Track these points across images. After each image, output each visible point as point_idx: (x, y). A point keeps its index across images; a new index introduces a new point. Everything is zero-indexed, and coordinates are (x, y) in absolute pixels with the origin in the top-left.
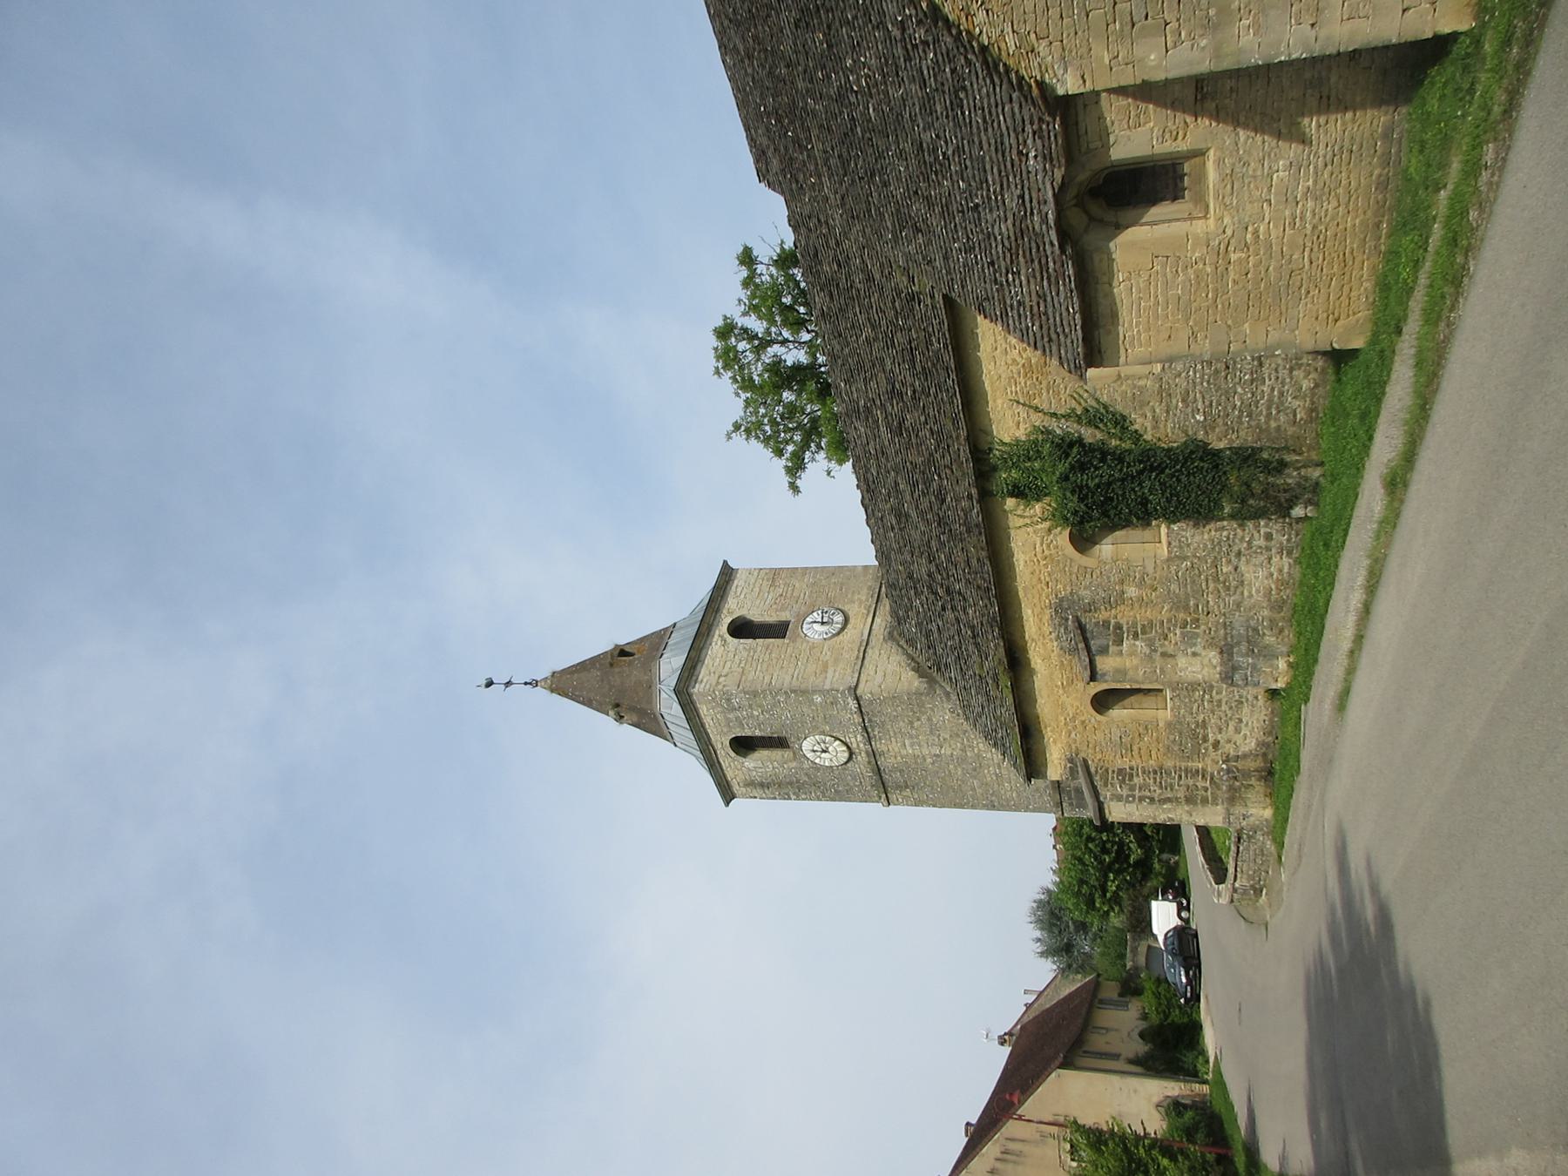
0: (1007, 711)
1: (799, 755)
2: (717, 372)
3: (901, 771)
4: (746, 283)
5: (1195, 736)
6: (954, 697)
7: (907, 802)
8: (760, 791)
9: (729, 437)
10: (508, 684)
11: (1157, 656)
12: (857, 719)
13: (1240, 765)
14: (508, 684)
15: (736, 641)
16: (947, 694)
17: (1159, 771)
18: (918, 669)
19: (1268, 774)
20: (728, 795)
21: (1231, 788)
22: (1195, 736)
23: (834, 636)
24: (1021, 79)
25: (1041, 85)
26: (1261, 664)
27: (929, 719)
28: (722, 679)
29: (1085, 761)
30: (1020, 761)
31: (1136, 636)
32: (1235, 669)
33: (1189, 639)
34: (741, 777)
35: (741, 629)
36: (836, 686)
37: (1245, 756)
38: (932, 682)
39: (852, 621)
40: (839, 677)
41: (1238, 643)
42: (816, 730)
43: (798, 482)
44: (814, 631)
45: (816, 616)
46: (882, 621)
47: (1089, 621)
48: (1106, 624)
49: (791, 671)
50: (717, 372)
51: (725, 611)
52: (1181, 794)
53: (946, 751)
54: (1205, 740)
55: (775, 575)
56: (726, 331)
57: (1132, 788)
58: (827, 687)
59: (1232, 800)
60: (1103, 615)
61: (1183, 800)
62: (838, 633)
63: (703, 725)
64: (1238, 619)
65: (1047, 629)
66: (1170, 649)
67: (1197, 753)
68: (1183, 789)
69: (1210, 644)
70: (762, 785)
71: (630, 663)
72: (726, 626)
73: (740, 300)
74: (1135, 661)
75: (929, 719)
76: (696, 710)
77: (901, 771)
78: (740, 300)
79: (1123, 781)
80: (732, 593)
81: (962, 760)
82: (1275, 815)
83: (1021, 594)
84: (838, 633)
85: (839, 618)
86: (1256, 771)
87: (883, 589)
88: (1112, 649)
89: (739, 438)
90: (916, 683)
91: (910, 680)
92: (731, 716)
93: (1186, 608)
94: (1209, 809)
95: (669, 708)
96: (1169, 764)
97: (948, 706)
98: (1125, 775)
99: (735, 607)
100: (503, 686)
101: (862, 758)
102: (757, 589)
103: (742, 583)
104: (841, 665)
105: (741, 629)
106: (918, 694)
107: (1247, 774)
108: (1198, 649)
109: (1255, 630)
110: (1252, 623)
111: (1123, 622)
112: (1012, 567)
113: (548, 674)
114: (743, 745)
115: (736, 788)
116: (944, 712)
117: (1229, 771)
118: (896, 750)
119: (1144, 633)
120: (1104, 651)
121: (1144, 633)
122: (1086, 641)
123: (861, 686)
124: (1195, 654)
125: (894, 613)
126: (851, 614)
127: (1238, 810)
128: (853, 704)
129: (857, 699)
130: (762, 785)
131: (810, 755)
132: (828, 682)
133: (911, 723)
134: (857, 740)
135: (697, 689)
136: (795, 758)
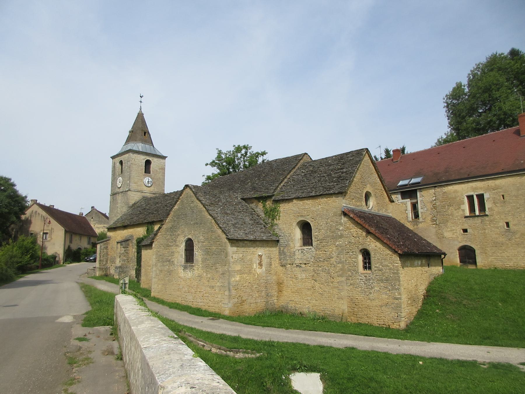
0: (119, 225)
1: (119, 176)
2: (234, 146)
3: (116, 199)
4: (258, 153)
5: (113, 261)
6: (127, 212)
7: (111, 200)
8: (113, 166)
9: (217, 149)
10: (141, 102)
11: (120, 255)
12: (124, 190)
13: (108, 270)
14: (141, 102)
15: (145, 162)
16: (128, 211)
17: (107, 254)
18: (135, 204)
19: (106, 275)
20: (113, 158)
21: (103, 268)
22: (113, 261)
23: (145, 185)
24: (154, 239)
25: (153, 242)
26: (118, 273)
27: (124, 206)
28: (134, 160)
29: (110, 240)
30: (110, 227)
31: (125, 251)
32: (117, 269)
33: (124, 260)
34: (116, 162)
35: (148, 163)
36: (131, 186)
37: (110, 271)
38: (131, 207)
39: (149, 188)
40: (133, 186)
41: (122, 269)
42: (123, 180)
43: (209, 166)
44: (146, 180)
45: (150, 180)
46: (148, 195)
47: (129, 242)
48: (129, 245)
49: (135, 175)
50: (234, 146)
51: (153, 158)
52: (102, 259)
53: (119, 209)
54: (113, 263)
55: (163, 169)
56: (245, 147)
57: (103, 249)
58: (131, 184)
59: (100, 268)
60: (131, 245)
61: (100, 259)
62: (145, 185)
63: (125, 154)
64: (128, 269)
65: (130, 233)
66: (121, 257)
67: (111, 262)
68: (103, 259)
69: (122, 264)
70: (114, 166)
71: (142, 135)
72: (148, 159)
73: (253, 152)
74: (119, 251)
75: (124, 206)
76: (127, 153)
77: (116, 199)
78: (253, 152)
79: (105, 247)
80: (158, 159)
81: (117, 212)
82: (97, 276)
83: (134, 229)
84: (145, 185)
85: (150, 185)
86: (107, 273)
87: (157, 195)
88: (122, 246)
89: (217, 152)
90: (131, 204)
91: (132, 202)
92: (126, 161)
93: (131, 260)
94: (98, 264)
95: (130, 146)
96: (109, 256)
97: (126, 210)
98: (106, 248)
99: (155, 162)
100: (140, 101)
101: (118, 190)
102: (159, 165)
103: (161, 161)
104: (136, 187)
105: (148, 163)
106: (128, 204)
107: (106, 271)
108: (121, 262)
109: (125, 272)
110: (127, 272)
111: (129, 248)
112: (138, 227)
113: (143, 112)
114: (121, 163)
115: (114, 160)
116: (125, 210)
117: (107, 268)
118: (119, 197)
119: (126, 252)
120: (121, 245)
121: (126, 252)
122: (124, 241)
123: (131, 192)
124: (120, 262)
125: (151, 198)
126: (151, 188)
127: (98, 270)
128: (127, 190)
129: (128, 191)
130: (114, 166)
131: (119, 179)
132: (132, 184)
133: (123, 202)
134: (121, 190)
135: (131, 154)
136: (119, 175)
